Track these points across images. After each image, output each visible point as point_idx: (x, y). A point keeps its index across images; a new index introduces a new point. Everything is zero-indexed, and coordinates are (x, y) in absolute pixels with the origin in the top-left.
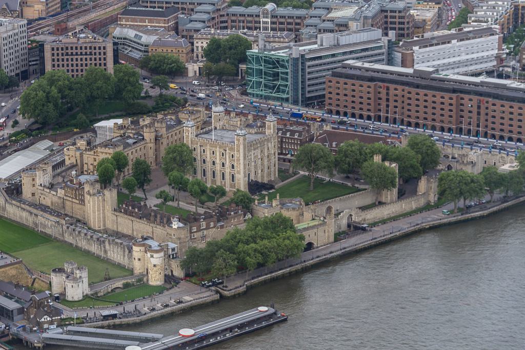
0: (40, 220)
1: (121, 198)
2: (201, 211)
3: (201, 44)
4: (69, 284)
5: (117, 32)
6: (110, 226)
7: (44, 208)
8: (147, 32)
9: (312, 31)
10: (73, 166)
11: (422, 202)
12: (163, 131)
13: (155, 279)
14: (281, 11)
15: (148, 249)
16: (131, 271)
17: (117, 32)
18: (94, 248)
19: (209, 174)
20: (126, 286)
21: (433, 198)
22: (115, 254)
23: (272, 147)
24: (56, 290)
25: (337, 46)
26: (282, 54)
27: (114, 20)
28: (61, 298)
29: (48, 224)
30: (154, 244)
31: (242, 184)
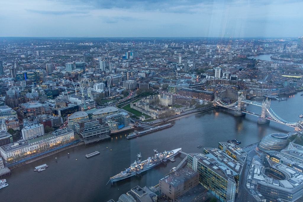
0: (138, 109)
1: (150, 106)
2: (161, 108)
3: (162, 85)
4: (142, 118)
5: (149, 83)
6: (148, 110)
7: (139, 108)
8: (153, 82)
9: (178, 83)
10: (143, 102)
11: (193, 108)
12: (156, 97)
13: (155, 118)
14: (173, 80)
15: (154, 114)
16: (151, 117)
17: (149, 83)
18: (146, 113)
19: (162, 103)
20: (150, 119)
21: (195, 108)
22: (149, 114)
23: (172, 100)
24: (140, 119)
25: (181, 85)
26: (173, 87)
27: (149, 81)
28: (141, 120)
29: (139, 110)
30: (155, 113)
31: (167, 105)
